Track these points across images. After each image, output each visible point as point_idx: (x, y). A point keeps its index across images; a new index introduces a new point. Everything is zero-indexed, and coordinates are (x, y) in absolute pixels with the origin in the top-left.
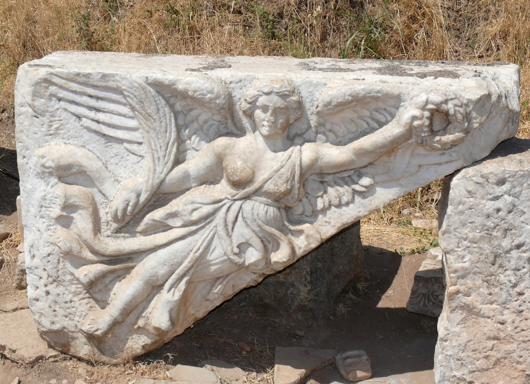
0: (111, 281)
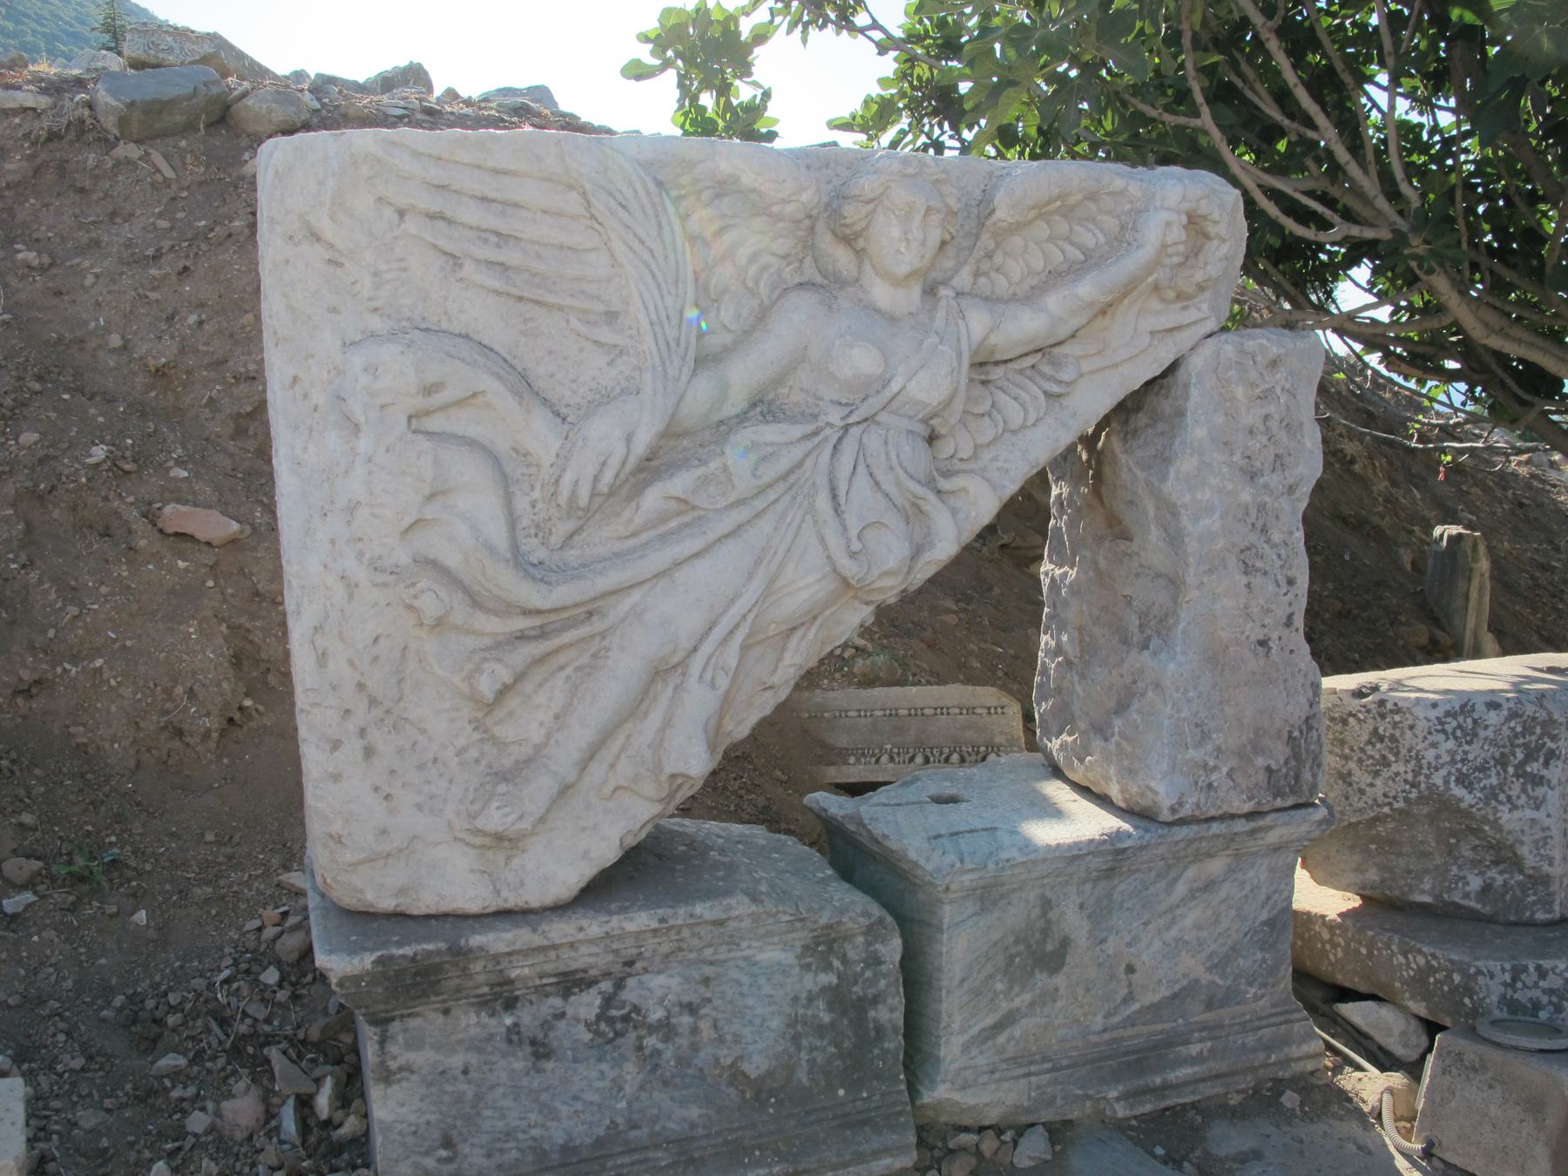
0: (540, 685)
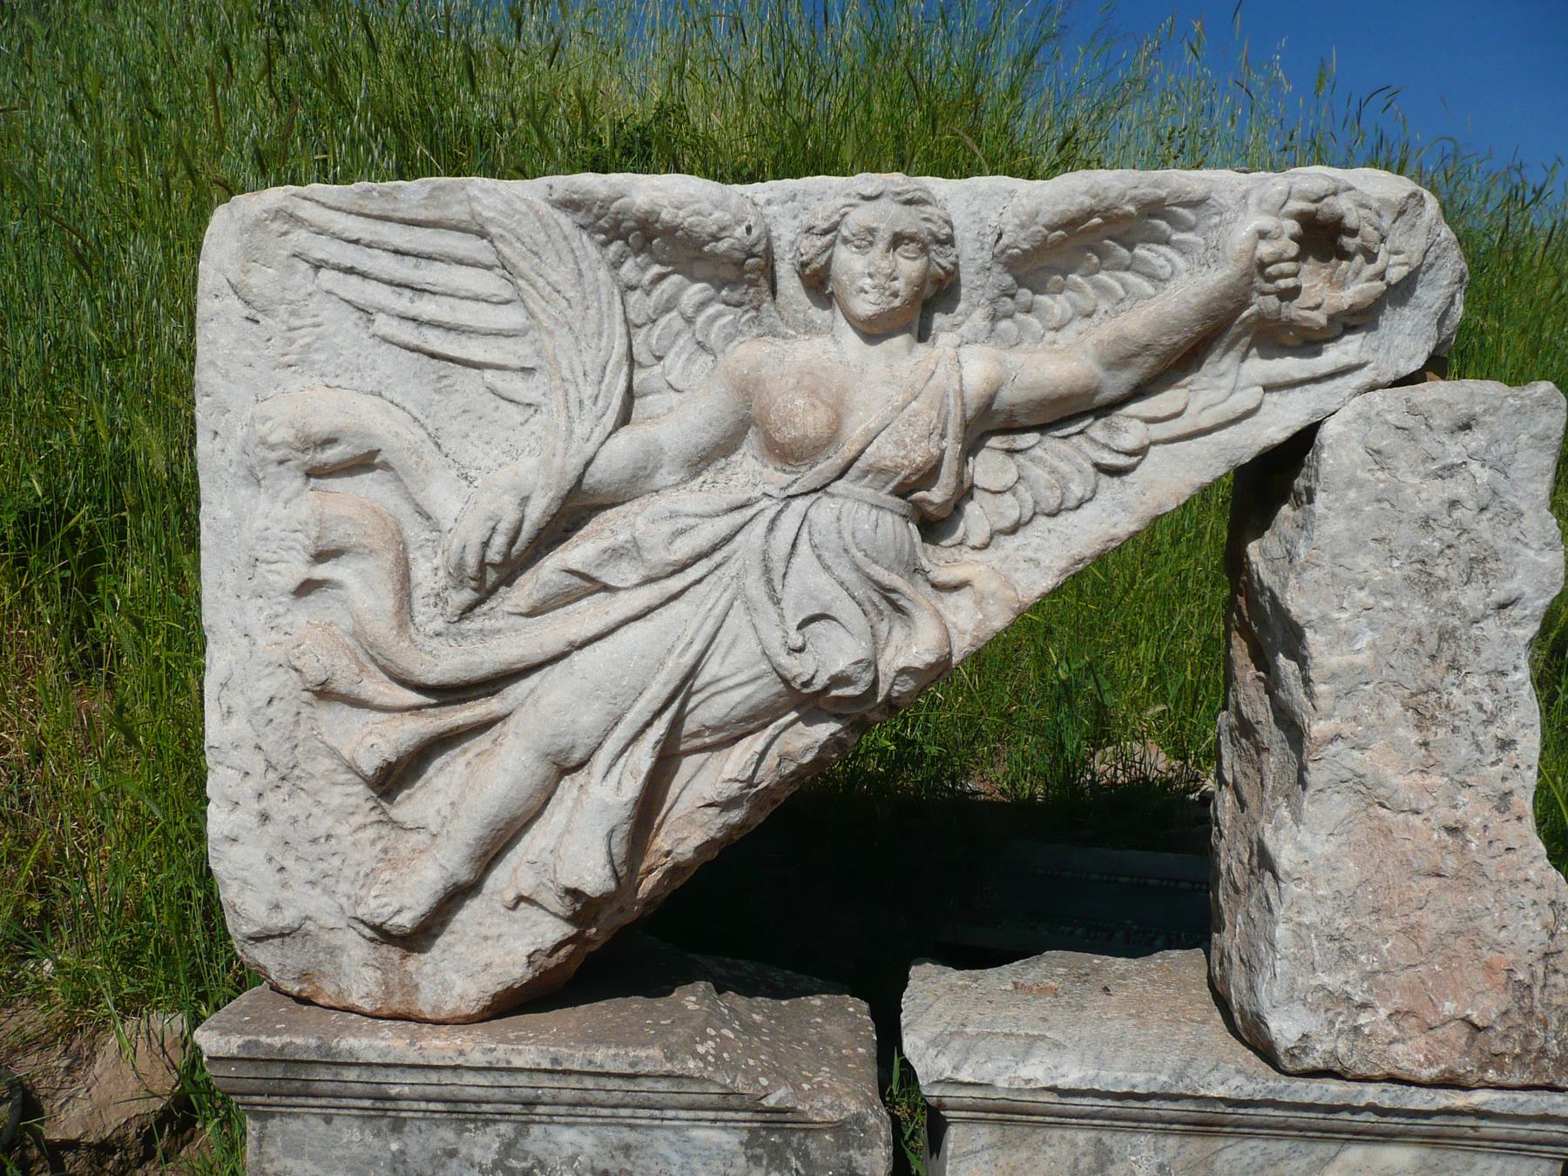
0: (441, 769)
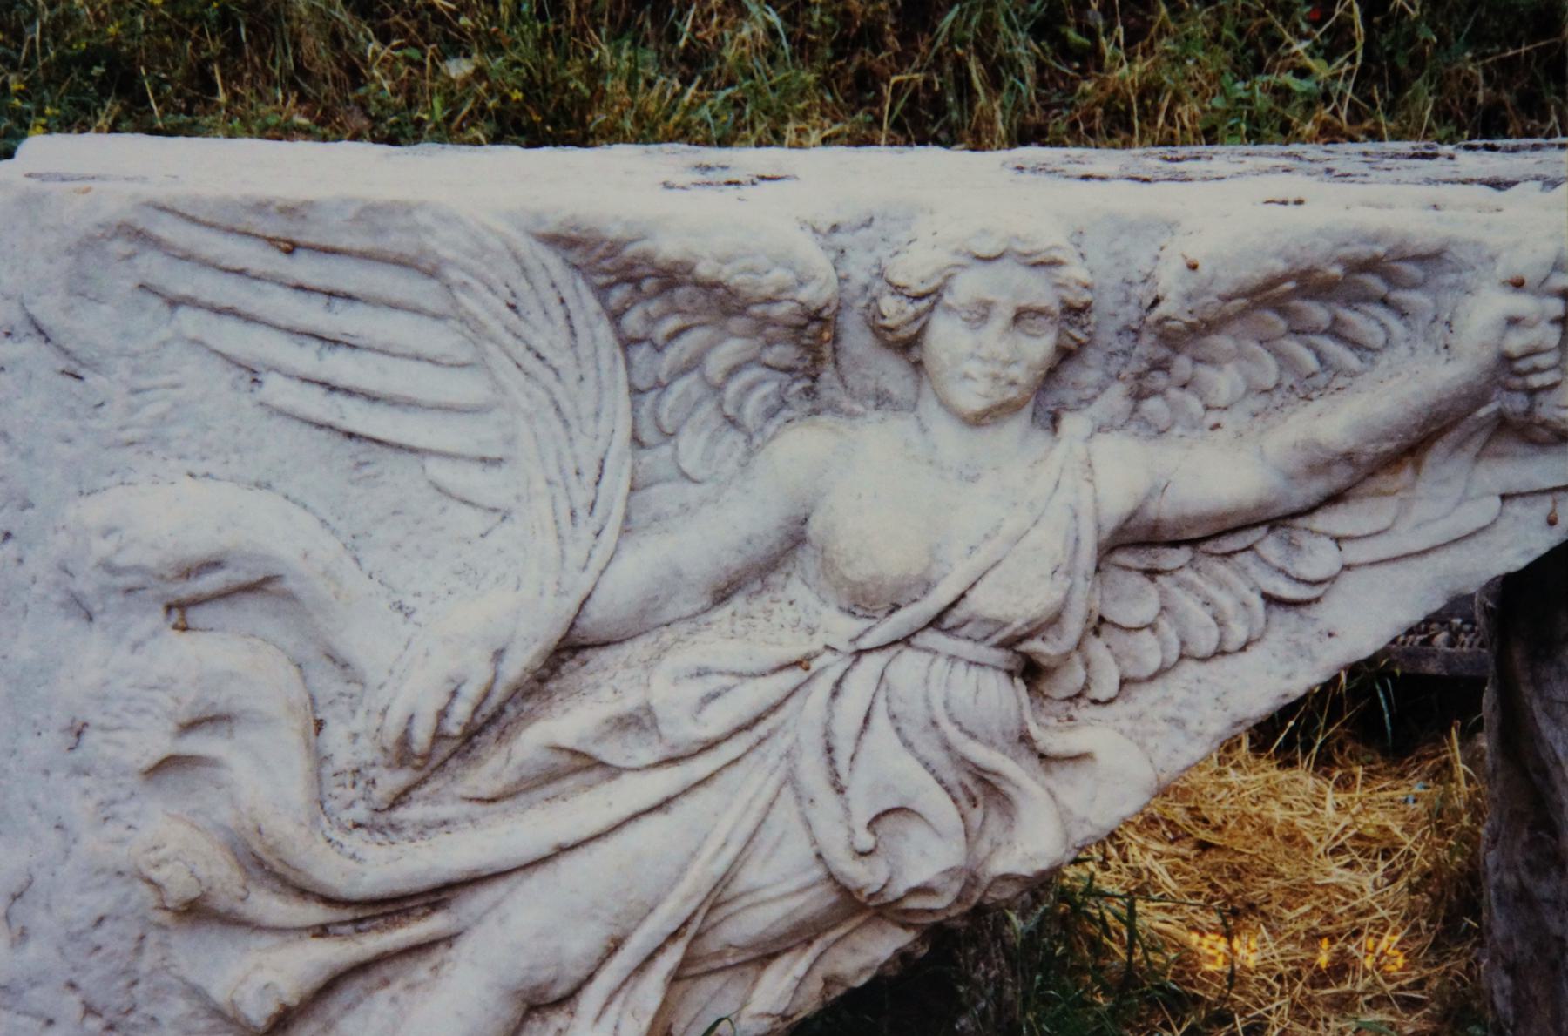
0: (350, 1007)
